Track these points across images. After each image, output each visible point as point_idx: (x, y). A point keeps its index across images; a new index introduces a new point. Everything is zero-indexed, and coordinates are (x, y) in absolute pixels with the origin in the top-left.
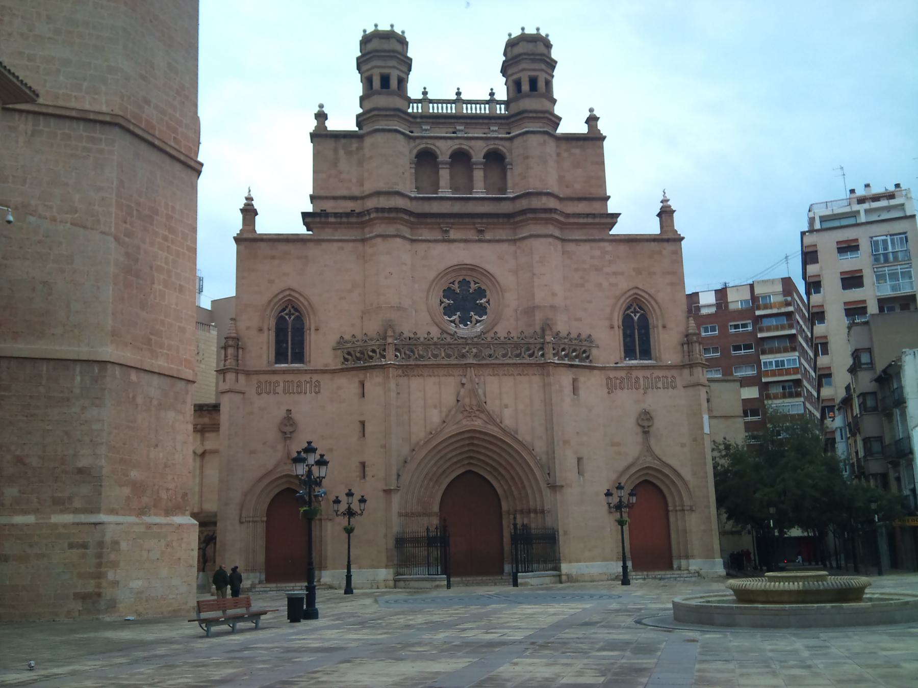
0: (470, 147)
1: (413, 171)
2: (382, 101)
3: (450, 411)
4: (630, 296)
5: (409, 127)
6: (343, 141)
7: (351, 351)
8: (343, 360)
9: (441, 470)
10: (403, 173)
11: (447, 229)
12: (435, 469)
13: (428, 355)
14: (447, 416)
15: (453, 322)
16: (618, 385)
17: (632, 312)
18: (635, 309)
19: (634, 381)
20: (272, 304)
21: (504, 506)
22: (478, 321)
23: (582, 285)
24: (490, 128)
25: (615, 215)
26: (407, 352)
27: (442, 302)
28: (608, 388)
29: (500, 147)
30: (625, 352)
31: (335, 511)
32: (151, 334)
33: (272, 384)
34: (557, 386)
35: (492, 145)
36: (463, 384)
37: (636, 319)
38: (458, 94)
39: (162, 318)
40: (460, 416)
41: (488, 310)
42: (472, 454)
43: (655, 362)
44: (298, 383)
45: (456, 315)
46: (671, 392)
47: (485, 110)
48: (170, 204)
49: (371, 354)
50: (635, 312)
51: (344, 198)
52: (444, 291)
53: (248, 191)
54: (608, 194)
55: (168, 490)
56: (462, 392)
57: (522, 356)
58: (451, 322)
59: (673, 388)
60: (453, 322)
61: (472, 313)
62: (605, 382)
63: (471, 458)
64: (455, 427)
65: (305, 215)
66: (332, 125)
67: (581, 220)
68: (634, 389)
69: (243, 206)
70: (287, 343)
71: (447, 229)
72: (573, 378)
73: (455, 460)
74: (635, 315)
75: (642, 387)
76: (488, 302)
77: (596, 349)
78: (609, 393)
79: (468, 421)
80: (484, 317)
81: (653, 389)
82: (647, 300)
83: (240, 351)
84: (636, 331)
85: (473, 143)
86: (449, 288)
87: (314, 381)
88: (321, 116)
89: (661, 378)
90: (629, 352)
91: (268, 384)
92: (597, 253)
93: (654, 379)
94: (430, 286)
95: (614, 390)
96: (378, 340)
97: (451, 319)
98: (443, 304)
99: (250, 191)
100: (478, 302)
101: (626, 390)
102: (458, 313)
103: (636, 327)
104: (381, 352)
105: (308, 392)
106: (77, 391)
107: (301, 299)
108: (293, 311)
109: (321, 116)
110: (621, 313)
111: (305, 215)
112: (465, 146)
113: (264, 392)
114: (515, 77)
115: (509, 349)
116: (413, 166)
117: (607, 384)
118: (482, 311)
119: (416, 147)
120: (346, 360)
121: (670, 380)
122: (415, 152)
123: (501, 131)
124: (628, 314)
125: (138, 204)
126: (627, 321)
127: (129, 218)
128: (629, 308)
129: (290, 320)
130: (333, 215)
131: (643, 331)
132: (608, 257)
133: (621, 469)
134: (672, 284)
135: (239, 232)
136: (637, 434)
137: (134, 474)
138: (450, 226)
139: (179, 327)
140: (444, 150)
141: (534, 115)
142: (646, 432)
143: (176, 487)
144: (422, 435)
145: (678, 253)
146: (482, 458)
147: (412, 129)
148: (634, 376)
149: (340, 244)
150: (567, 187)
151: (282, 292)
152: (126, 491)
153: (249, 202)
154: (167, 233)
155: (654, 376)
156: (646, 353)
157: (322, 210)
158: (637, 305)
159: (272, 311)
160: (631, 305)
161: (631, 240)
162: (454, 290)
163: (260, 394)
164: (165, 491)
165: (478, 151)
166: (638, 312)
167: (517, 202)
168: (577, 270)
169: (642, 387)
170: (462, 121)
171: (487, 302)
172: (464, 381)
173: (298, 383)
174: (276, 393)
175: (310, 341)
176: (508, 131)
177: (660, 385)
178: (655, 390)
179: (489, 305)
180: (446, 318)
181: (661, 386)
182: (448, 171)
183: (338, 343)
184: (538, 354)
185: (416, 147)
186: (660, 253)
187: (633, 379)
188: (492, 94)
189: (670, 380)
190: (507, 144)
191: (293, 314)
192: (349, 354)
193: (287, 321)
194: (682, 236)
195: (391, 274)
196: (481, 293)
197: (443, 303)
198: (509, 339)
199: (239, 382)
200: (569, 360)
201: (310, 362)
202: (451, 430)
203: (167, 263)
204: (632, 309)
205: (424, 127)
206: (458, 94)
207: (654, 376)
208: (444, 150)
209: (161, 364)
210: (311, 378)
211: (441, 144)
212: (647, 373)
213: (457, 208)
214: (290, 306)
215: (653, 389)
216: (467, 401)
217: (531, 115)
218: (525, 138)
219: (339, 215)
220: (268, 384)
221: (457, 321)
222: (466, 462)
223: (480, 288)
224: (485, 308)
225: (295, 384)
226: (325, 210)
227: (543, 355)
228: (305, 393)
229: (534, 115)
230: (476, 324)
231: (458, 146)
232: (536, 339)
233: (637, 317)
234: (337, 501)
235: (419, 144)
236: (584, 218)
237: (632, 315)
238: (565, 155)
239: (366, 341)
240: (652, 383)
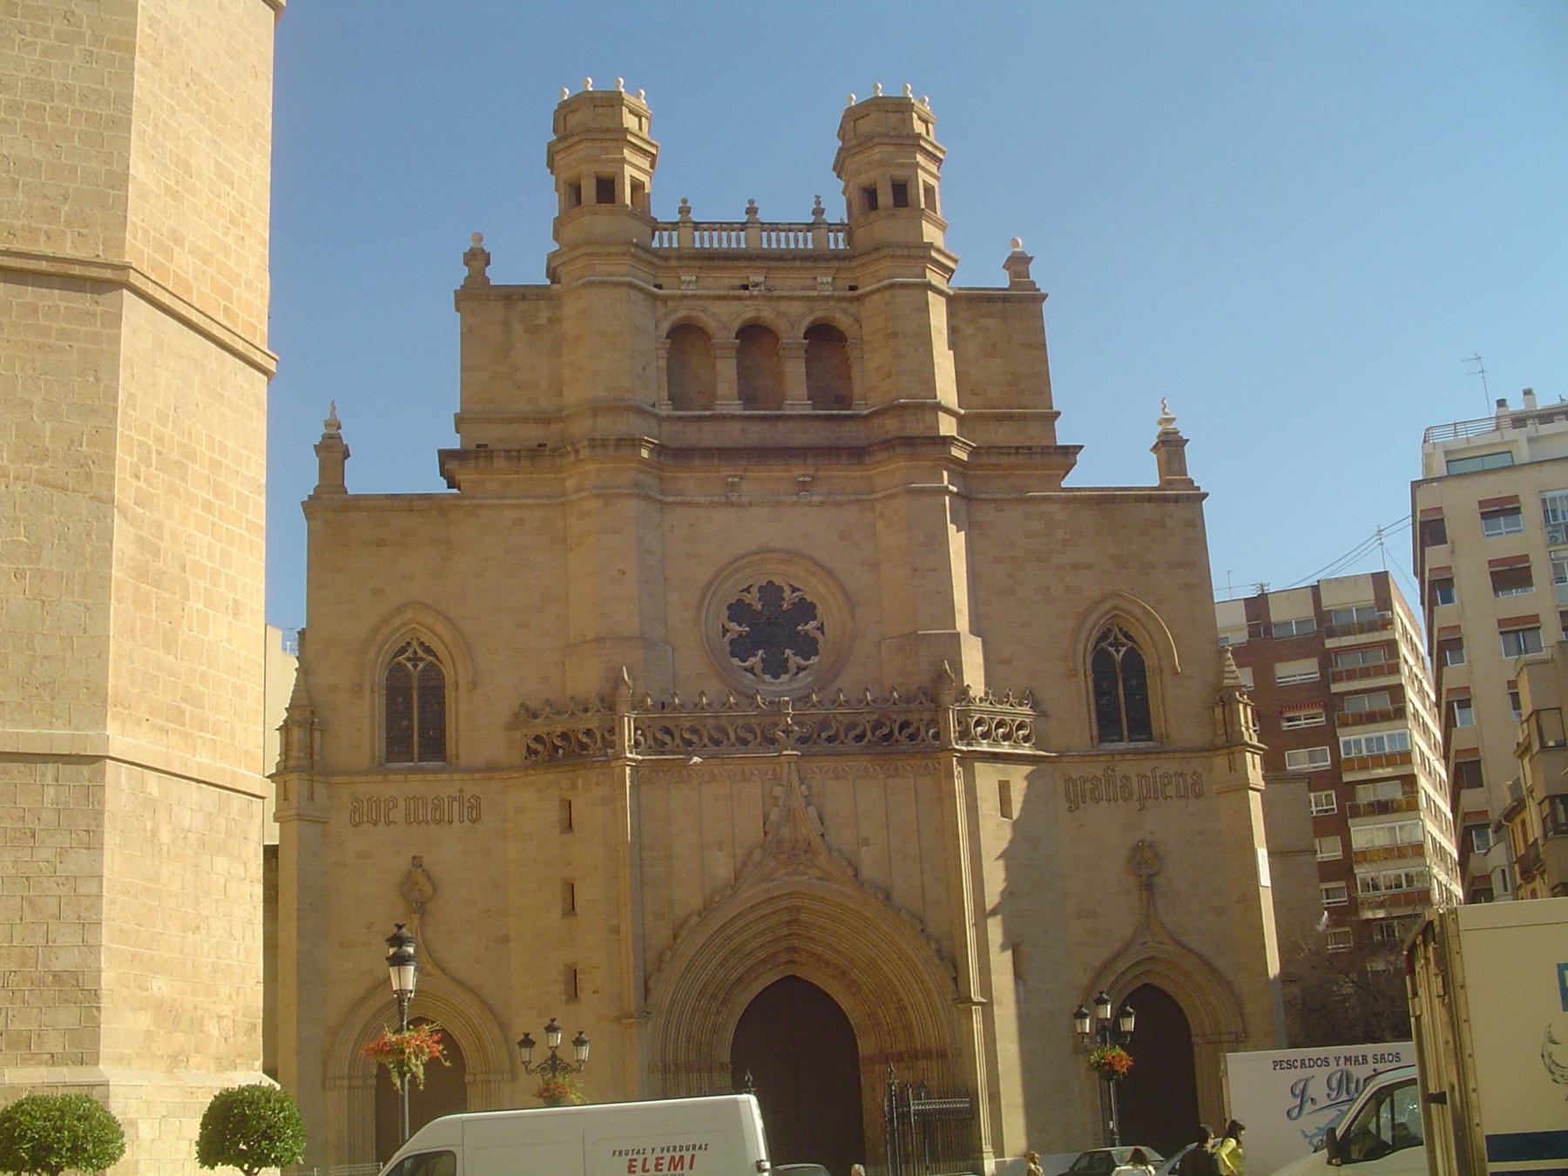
0: (779, 314)
1: (663, 363)
2: (600, 222)
3: (750, 854)
4: (1106, 613)
5: (654, 277)
6: (523, 306)
7: (542, 731)
8: (525, 749)
9: (734, 976)
11: (735, 480)
12: (721, 973)
13: (701, 738)
14: (745, 864)
15: (751, 670)
17: (1110, 645)
18: (1116, 638)
19: (1119, 784)
20: (380, 638)
21: (865, 1046)
22: (800, 669)
24: (815, 279)
25: (1071, 450)
26: (659, 735)
27: (725, 631)
29: (838, 315)
30: (1101, 727)
31: (523, 1063)
32: (184, 700)
33: (382, 804)
35: (820, 313)
36: (776, 798)
37: (1119, 657)
38: (751, 211)
39: (204, 668)
40: (772, 863)
41: (821, 646)
42: (796, 943)
43: (1157, 744)
44: (435, 801)
45: (755, 655)
47: (806, 242)
48: (217, 438)
49: (585, 740)
50: (1117, 645)
51: (525, 420)
52: (730, 607)
53: (330, 408)
54: (1055, 409)
55: (220, 1017)
56: (774, 815)
57: (894, 739)
58: (746, 670)
59: (1199, 796)
60: (751, 670)
61: (788, 652)
62: (1061, 788)
63: (795, 950)
64: (764, 886)
65: (445, 456)
66: (498, 275)
67: (1005, 460)
68: (1121, 801)
69: (320, 439)
70: (411, 720)
71: (735, 480)
72: (999, 781)
73: (761, 954)
74: (1118, 651)
75: (1136, 797)
76: (821, 628)
79: (787, 874)
80: (814, 660)
81: (1156, 799)
82: (1138, 620)
83: (317, 735)
84: (1120, 684)
86: (740, 601)
87: (467, 797)
88: (477, 258)
91: (374, 805)
94: (704, 595)
95: (1081, 805)
96: (599, 711)
97: (747, 664)
98: (729, 634)
99: (334, 408)
100: (800, 628)
101: (1103, 804)
102: (761, 652)
103: (1120, 676)
104: (605, 733)
105: (456, 820)
106: (48, 817)
107: (439, 628)
108: (421, 653)
109: (477, 258)
110: (1090, 646)
111: (445, 456)
112: (767, 313)
113: (366, 819)
114: (864, 179)
115: (867, 725)
116: (663, 353)
117: (1067, 793)
118: (808, 647)
119: (666, 316)
120: (531, 752)
121: (1190, 781)
122: (666, 326)
123: (840, 283)
125: (160, 439)
126: (1102, 666)
127: (143, 468)
128: (1104, 636)
130: (502, 454)
131: (1134, 682)
135: (312, 493)
137: (159, 986)
138: (741, 473)
139: (234, 686)
140: (723, 319)
141: (905, 252)
142: (1149, 886)
143: (235, 1012)
144: (696, 903)
145: (1196, 525)
146: (819, 949)
147: (658, 282)
148: (1119, 775)
149: (517, 514)
150: (974, 393)
151: (400, 610)
152: (145, 1020)
153: (333, 431)
154: (210, 497)
155: (1159, 772)
156: (1141, 725)
157: (478, 446)
158: (1120, 629)
159: (379, 653)
160: (1109, 630)
161: (1106, 501)
162: (750, 605)
163: (357, 825)
164: (215, 1020)
165: (792, 321)
166: (1123, 646)
167: (876, 423)
169: (1136, 797)
170: (759, 264)
171: (818, 629)
172: (778, 790)
173: (435, 801)
174: (389, 823)
175: (457, 714)
176: (853, 284)
177: (1171, 790)
179: (823, 633)
180: (736, 661)
182: (733, 362)
183: (516, 716)
184: (927, 733)
185: (666, 316)
188: (818, 212)
189: (1190, 781)
190: (852, 308)
191: (421, 659)
192: (538, 739)
193: (409, 671)
194: (1203, 490)
195: (624, 574)
197: (728, 631)
198: (868, 704)
199: (316, 798)
200: (990, 745)
201: (458, 757)
202: (751, 893)
203: (211, 558)
205: (683, 278)
206: (751, 211)
207: (1159, 772)
208: (723, 319)
209: (201, 761)
210: (461, 790)
211: (721, 308)
212: (1146, 766)
213: (757, 434)
214: (415, 644)
215: (1156, 799)
216: (786, 832)
217: (898, 252)
218: (888, 294)
219: (515, 454)
220: (374, 805)
221: (758, 670)
222: (784, 958)
224: (815, 641)
225: (430, 803)
226: (486, 446)
227: (936, 736)
228: (451, 822)
229: (905, 252)
230: (797, 674)
231: (753, 314)
232: (921, 703)
233: (1121, 654)
234: (527, 1042)
235: (675, 310)
236: (1009, 454)
237: (1112, 650)
238: (967, 330)
239: (573, 713)
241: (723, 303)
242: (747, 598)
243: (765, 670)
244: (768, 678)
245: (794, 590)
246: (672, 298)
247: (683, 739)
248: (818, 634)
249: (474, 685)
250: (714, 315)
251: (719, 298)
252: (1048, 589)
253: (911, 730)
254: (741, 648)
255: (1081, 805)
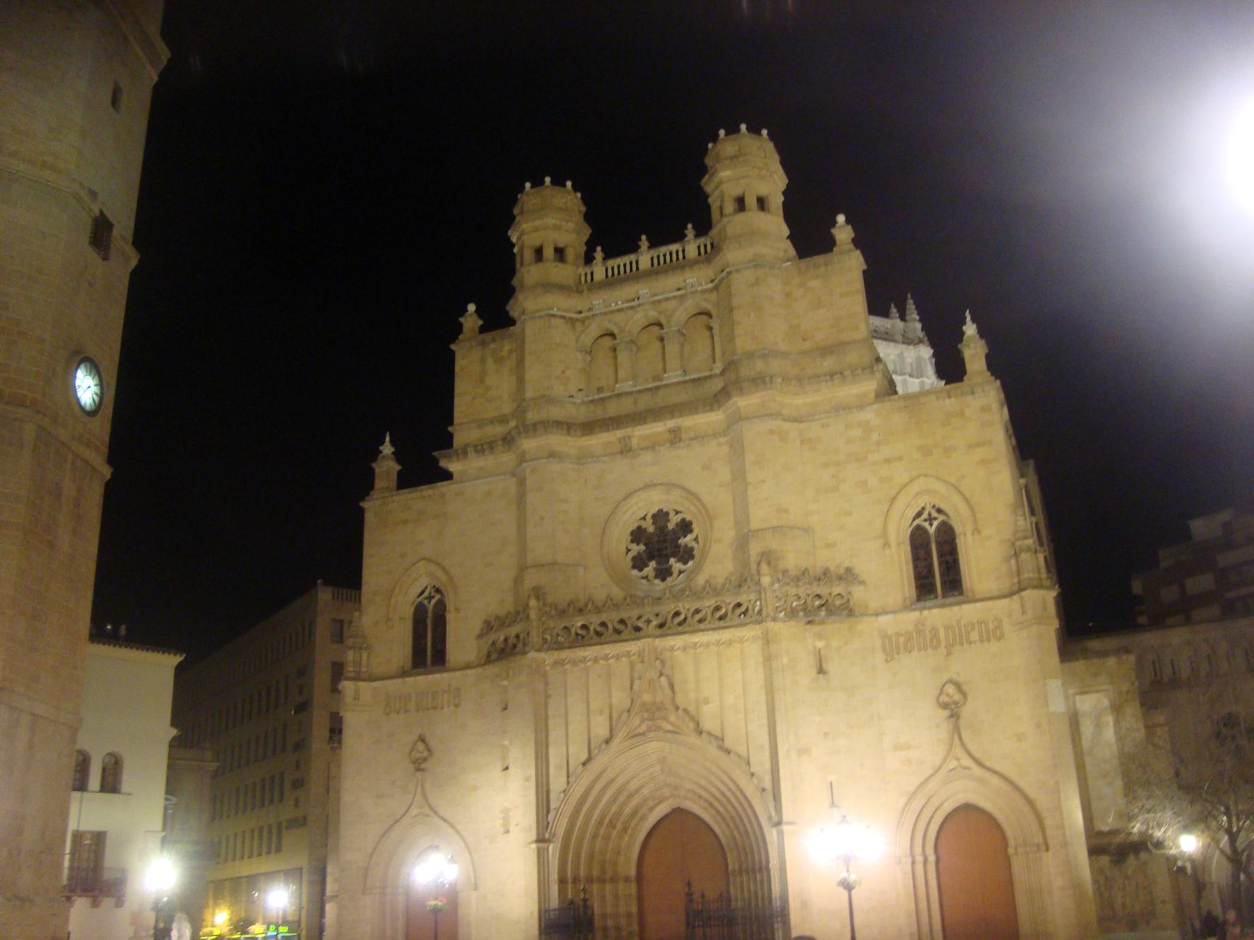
10: (563, 372)
15: (646, 578)
16: (902, 646)
17: (926, 520)
18: (930, 514)
22: (680, 572)
23: (835, 489)
27: (628, 550)
28: (887, 655)
34: (785, 660)
46: (994, 646)
50: (930, 519)
58: (643, 578)
59: (999, 639)
60: (646, 578)
61: (672, 560)
62: (878, 643)
68: (929, 650)
74: (931, 525)
75: (943, 643)
77: (861, 588)
78: (887, 661)
80: (690, 563)
81: (962, 644)
85: (664, 306)
89: (976, 626)
90: (924, 587)
92: (856, 432)
93: (963, 629)
100: (680, 541)
101: (915, 653)
118: (687, 555)
121: (991, 627)
124: (919, 527)
128: (919, 515)
129: (431, 606)
130: (472, 449)
132: (875, 437)
133: (912, 789)
134: (984, 462)
136: (938, 726)
150: (804, 340)
156: (953, 583)
168: (826, 465)
178: (966, 646)
179: (698, 543)
180: (635, 572)
181: (977, 638)
186: (961, 414)
187: (928, 634)
189: (991, 627)
196: (686, 527)
204: (925, 515)
223: (683, 520)
237: (926, 525)
240: (961, 636)
241: (622, 314)
242: (644, 524)
243: (656, 577)
244: (657, 581)
245: (677, 513)
246: (588, 318)
247: (577, 634)
248: (694, 544)
249: (457, 610)
250: (615, 324)
251: (619, 310)
252: (864, 483)
253: (743, 609)
254: (639, 563)
255: (896, 656)
